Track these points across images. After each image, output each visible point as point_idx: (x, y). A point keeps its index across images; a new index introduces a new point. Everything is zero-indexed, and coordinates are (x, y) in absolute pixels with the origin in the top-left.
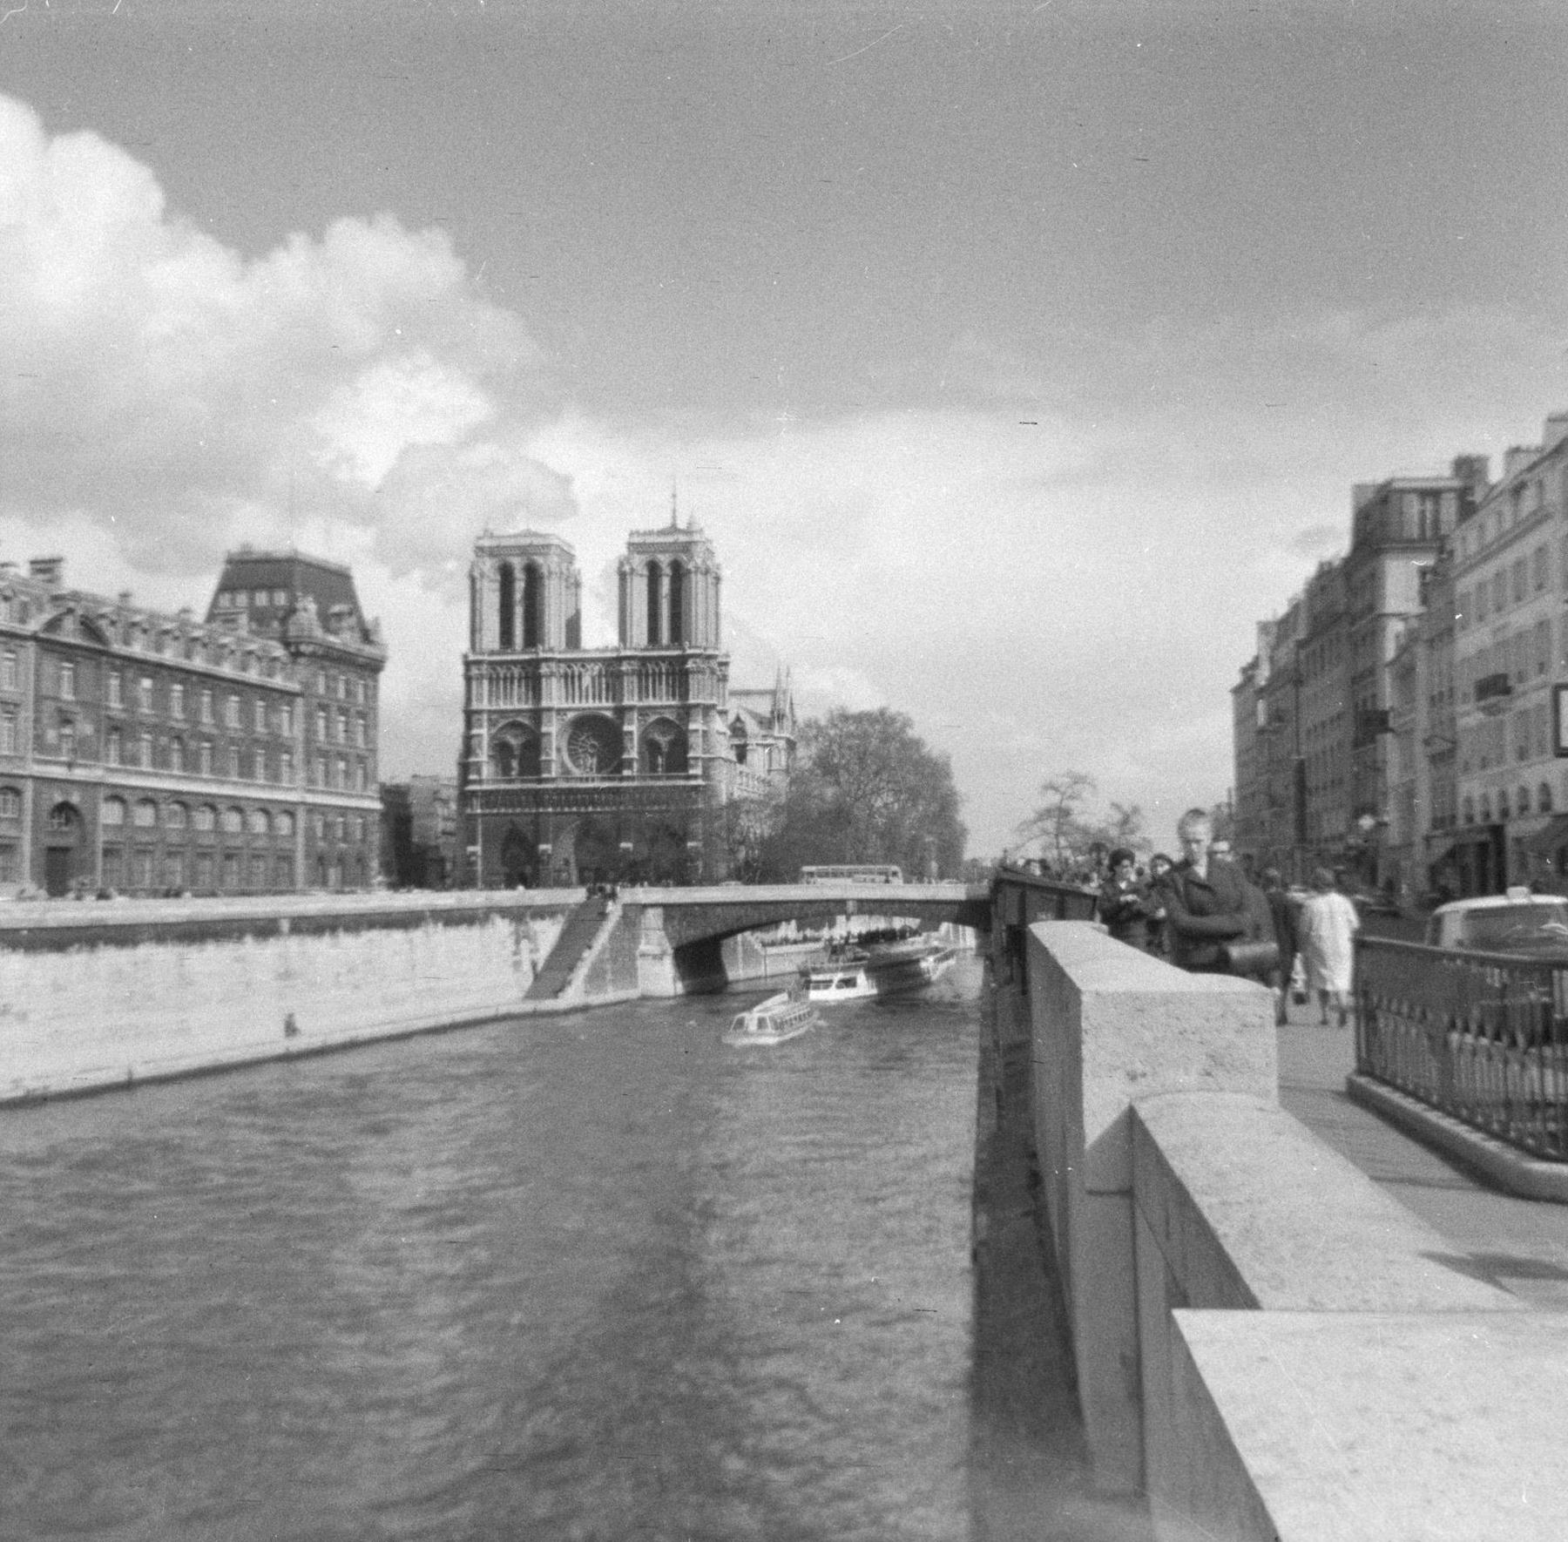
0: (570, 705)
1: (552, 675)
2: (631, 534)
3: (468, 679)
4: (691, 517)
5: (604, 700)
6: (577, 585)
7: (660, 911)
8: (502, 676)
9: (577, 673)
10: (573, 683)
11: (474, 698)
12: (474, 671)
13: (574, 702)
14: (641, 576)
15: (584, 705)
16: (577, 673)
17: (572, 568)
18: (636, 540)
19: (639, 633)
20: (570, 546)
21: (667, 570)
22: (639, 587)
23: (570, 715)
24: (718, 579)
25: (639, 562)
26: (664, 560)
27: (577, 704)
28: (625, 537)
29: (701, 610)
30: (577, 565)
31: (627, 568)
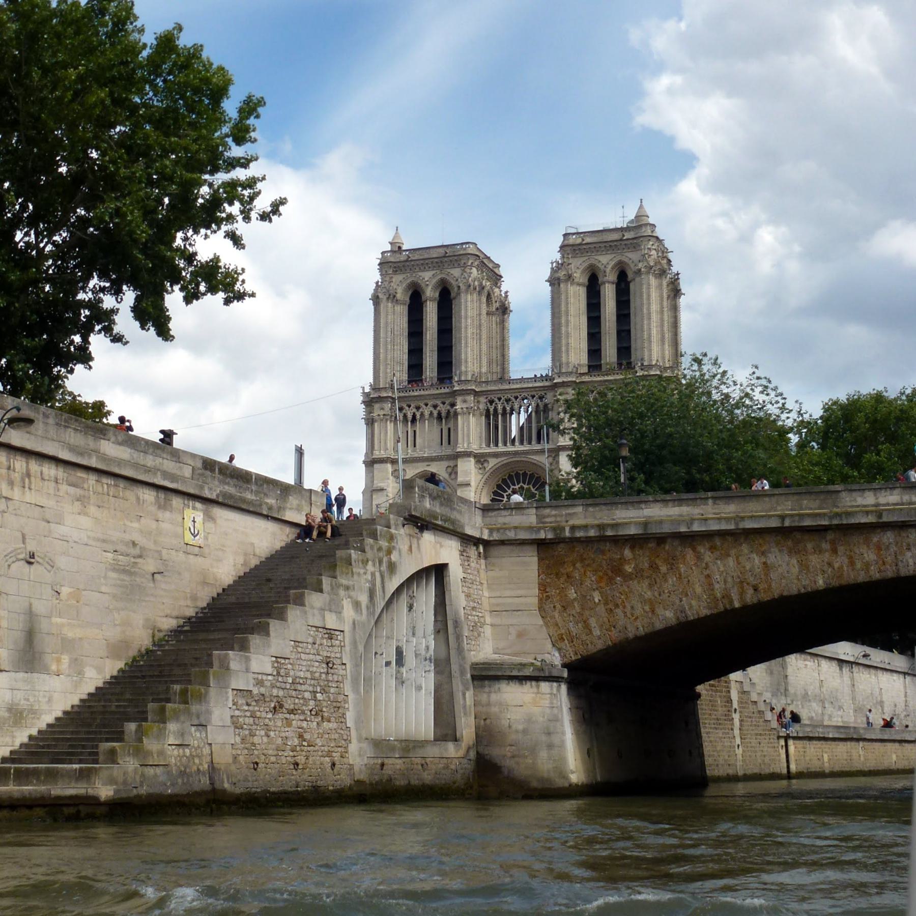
0: (493, 449)
1: (469, 411)
2: (565, 235)
3: (370, 422)
4: (641, 207)
5: (534, 442)
6: (504, 310)
7: (530, 561)
8: (410, 417)
9: (500, 411)
10: (496, 428)
11: (376, 447)
12: (377, 411)
13: (497, 445)
14: (579, 284)
15: (510, 448)
16: (500, 411)
17: (496, 290)
18: (572, 240)
19: (578, 354)
20: (498, 266)
21: (612, 277)
22: (577, 297)
23: (492, 463)
24: (676, 292)
25: (578, 269)
26: (606, 262)
27: (501, 448)
28: (560, 240)
29: (654, 331)
30: (504, 288)
31: (561, 274)
